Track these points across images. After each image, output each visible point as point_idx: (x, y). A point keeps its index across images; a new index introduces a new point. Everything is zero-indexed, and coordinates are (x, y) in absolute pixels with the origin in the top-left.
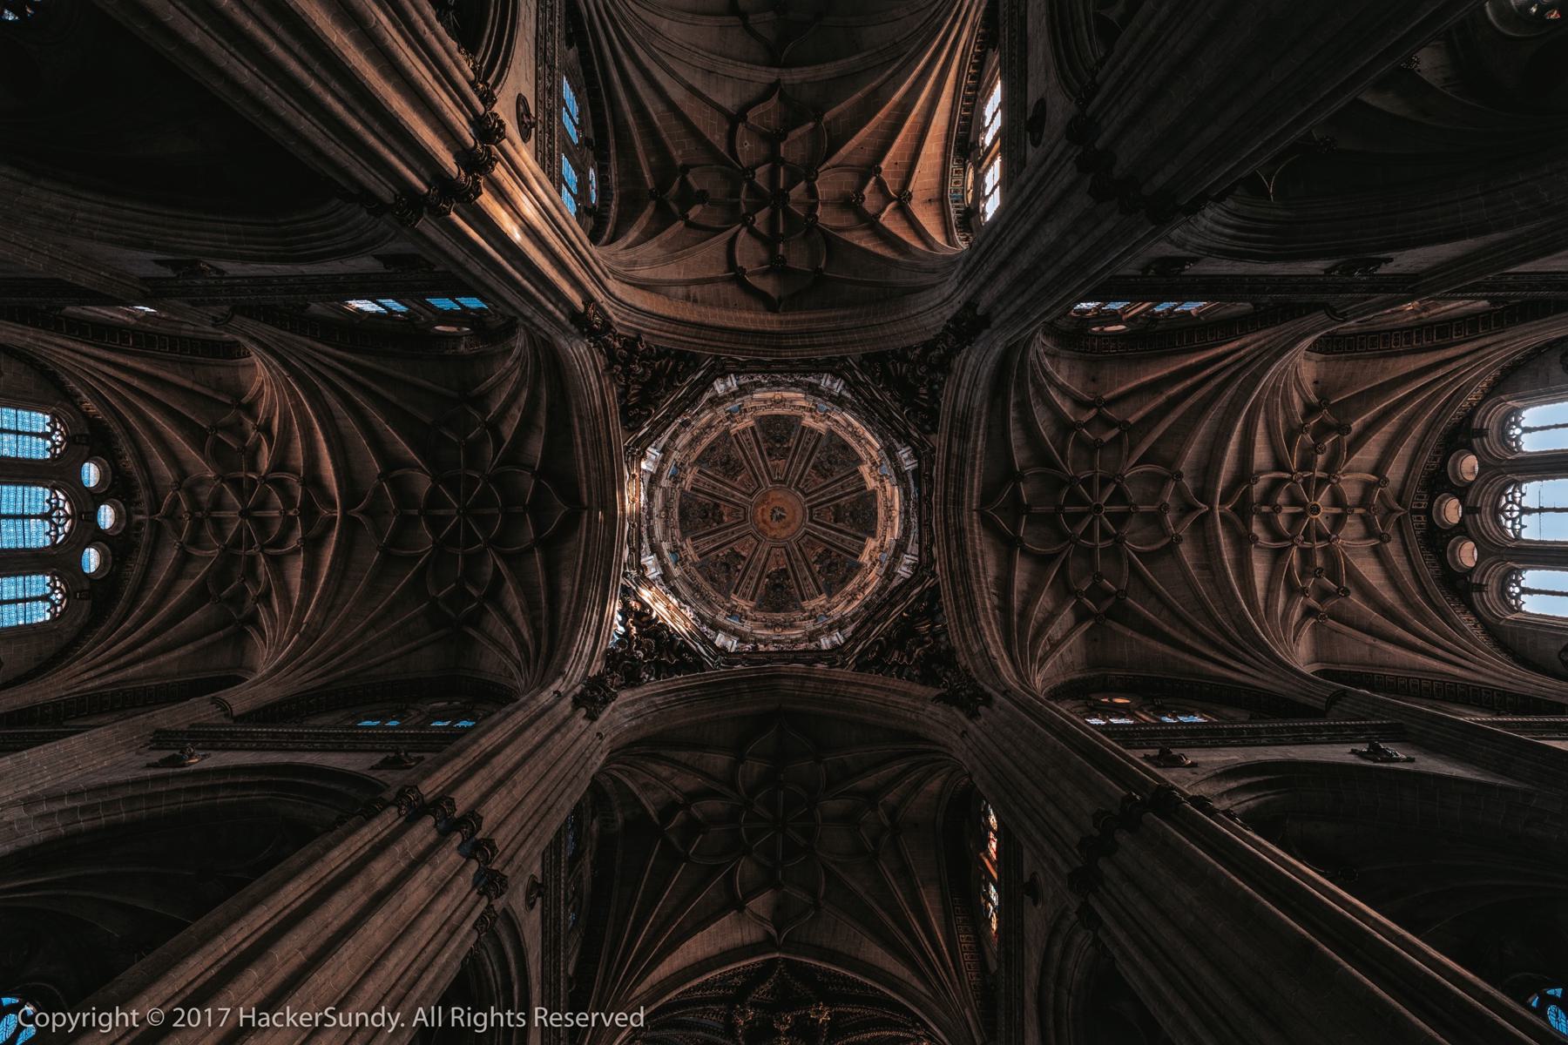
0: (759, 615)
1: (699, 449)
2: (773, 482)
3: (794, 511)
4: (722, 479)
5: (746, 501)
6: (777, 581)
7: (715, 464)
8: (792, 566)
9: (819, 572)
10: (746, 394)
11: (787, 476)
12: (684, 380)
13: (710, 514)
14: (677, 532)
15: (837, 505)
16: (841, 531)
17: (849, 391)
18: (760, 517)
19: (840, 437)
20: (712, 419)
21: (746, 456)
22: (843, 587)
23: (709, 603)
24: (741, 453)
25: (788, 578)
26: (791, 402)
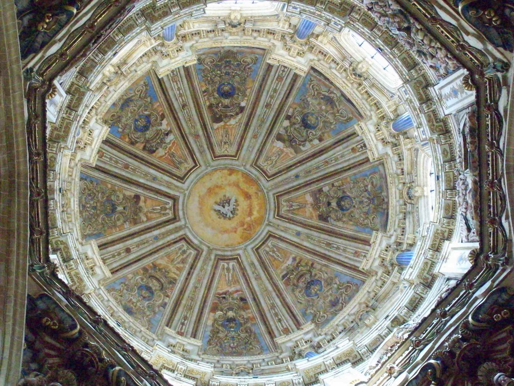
0: (262, 42)
1: (361, 296)
2: (236, 259)
4: (317, 259)
6: (226, 101)
7: (329, 282)
8: (204, 126)
9: (163, 117)
12: (424, 369)
13: (334, 204)
14: (392, 167)
15: (135, 222)
18: (255, 203)
21: (280, 295)
23: (344, 58)
24: (289, 299)
25: (210, 107)
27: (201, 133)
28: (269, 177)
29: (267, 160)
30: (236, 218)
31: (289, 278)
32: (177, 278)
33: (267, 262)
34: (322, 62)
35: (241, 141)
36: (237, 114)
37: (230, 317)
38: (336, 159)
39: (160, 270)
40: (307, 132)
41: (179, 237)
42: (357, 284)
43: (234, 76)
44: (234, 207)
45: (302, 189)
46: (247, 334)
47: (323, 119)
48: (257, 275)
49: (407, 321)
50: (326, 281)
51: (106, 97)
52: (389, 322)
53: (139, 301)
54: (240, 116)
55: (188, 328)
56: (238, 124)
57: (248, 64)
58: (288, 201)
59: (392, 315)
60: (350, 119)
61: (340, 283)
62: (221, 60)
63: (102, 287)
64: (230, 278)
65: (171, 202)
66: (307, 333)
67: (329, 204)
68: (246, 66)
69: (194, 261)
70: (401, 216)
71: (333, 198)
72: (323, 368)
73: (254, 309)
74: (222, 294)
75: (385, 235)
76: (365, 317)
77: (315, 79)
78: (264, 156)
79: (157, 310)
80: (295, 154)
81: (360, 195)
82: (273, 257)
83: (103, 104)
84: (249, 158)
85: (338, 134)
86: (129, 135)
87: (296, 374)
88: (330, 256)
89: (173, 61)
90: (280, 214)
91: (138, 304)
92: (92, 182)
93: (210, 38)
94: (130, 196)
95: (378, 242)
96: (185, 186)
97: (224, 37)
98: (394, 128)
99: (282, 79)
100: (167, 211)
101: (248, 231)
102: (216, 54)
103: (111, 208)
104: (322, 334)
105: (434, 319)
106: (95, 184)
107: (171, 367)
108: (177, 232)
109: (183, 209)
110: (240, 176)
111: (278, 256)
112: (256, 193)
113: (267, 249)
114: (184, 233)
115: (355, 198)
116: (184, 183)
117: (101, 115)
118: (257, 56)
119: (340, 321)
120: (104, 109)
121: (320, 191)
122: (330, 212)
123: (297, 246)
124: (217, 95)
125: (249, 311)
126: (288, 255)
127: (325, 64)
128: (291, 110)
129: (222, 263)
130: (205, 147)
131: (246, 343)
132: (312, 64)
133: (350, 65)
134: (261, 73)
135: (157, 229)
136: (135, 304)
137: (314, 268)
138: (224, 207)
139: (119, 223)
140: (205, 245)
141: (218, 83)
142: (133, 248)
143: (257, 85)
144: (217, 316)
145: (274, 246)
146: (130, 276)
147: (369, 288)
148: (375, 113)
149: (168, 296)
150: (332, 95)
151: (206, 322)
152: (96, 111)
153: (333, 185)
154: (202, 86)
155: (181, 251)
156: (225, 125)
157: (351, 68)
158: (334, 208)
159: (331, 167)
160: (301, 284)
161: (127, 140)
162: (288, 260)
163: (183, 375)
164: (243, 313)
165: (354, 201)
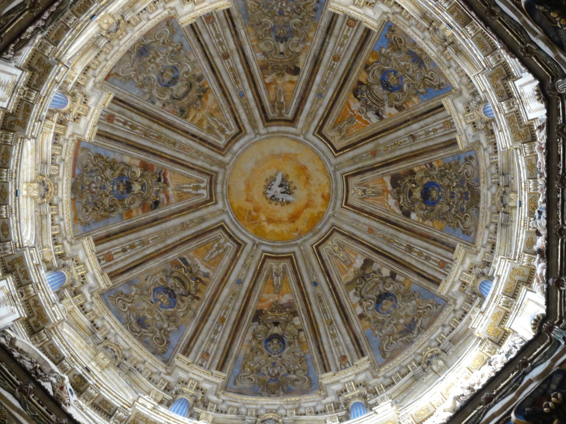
0: (483, 237)
2: (211, 200)
3: (274, 156)
4: (204, 305)
5: (251, 255)
6: (417, 194)
7: (171, 318)
8: (387, 164)
9: (400, 108)
10: (21, 260)
11: (201, 171)
13: (276, 330)
15: (263, 68)
16: (317, 62)
17: (17, 50)
18: (284, 228)
19: (120, 62)
20: (76, 326)
22: (430, 59)
23: (453, 342)
24: (152, 264)
25: (412, 173)
26: (44, 163)
27: (379, 159)
28: (317, 247)
29: (340, 245)
30: (266, 202)
31: (181, 267)
32: (189, 120)
33: (204, 240)
34: (452, 315)
35: (366, 212)
36: (401, 208)
37: (132, 186)
38: (334, 336)
39: (200, 97)
40: (373, 299)
41: (243, 126)
42: (164, 353)
43: (448, 204)
44: (281, 200)
45: (298, 290)
46: (108, 206)
47: (387, 321)
48: (187, 226)
49: (79, 396)
50: (174, 314)
51: (416, 26)
52: (81, 372)
53: (157, 66)
54: (398, 211)
55: (120, 130)
56: (388, 209)
57: (462, 223)
58: (284, 272)
59: (89, 376)
60: (384, 356)
61: (169, 332)
62: (468, 184)
63: (166, 12)
64: (185, 190)
65: (290, 116)
66: (95, 279)
67: (276, 324)
68: (461, 220)
69: (210, 144)
70: (243, 410)
71: (284, 330)
72: (24, 281)
73: (143, 218)
74: (165, 179)
75: (220, 387)
76: (108, 353)
77: (438, 310)
78: (345, 241)
79: (146, 90)
80: (345, 283)
81: (284, 365)
82: (212, 247)
83: (407, 22)
84: (342, 221)
85: (367, 339)
86: (376, 62)
87: (18, 246)
88: (207, 321)
89: (461, 117)
90: (268, 260)
91: (153, 65)
92: (315, 10)
93: (490, 167)
94: (298, 62)
95: (210, 378)
96: (310, 136)
97: (491, 187)
98: (357, 404)
99: (442, 267)
100: (277, 110)
101: (248, 216)
102: (478, 181)
103: (282, 36)
104: (93, 298)
105: (57, 416)
106: (313, 15)
107: (34, 82)
108: (250, 121)
109: (279, 132)
110: (320, 209)
111: (212, 254)
112: (297, 230)
113: (222, 241)
114: (248, 132)
115: (280, 357)
116: (314, 135)
117: (394, 20)
118: (473, 235)
119: (108, 322)
120: (400, 22)
121: (295, 314)
122: (265, 325)
123: (223, 281)
124: (425, 181)
125: (140, 213)
126: (213, 268)
127: (449, 319)
128: (402, 279)
129: (206, 179)
130: (360, 165)
131: (95, 204)
132: (451, 302)
133: (443, 351)
134: (451, 240)
135: (254, 96)
136: (153, 60)
137: (192, 299)
138: (281, 186)
139: (262, 45)
140: (232, 158)
141: (441, 184)
142: (229, 63)
143: (436, 234)
144: (134, 169)
145: (225, 250)
146: (192, 58)
147: (150, 363)
148: (382, 382)
149: (164, 105)
150: (416, 332)
151: (129, 155)
152: (397, 13)
153: (300, 330)
154: (438, 161)
155: (224, 127)
156: (388, 191)
157: (439, 351)
158: (271, 331)
159: (325, 329)
160: (171, 282)
161: (371, 60)
162: (206, 267)
163: (22, 97)
164: (138, 203)
165: (276, 356)
